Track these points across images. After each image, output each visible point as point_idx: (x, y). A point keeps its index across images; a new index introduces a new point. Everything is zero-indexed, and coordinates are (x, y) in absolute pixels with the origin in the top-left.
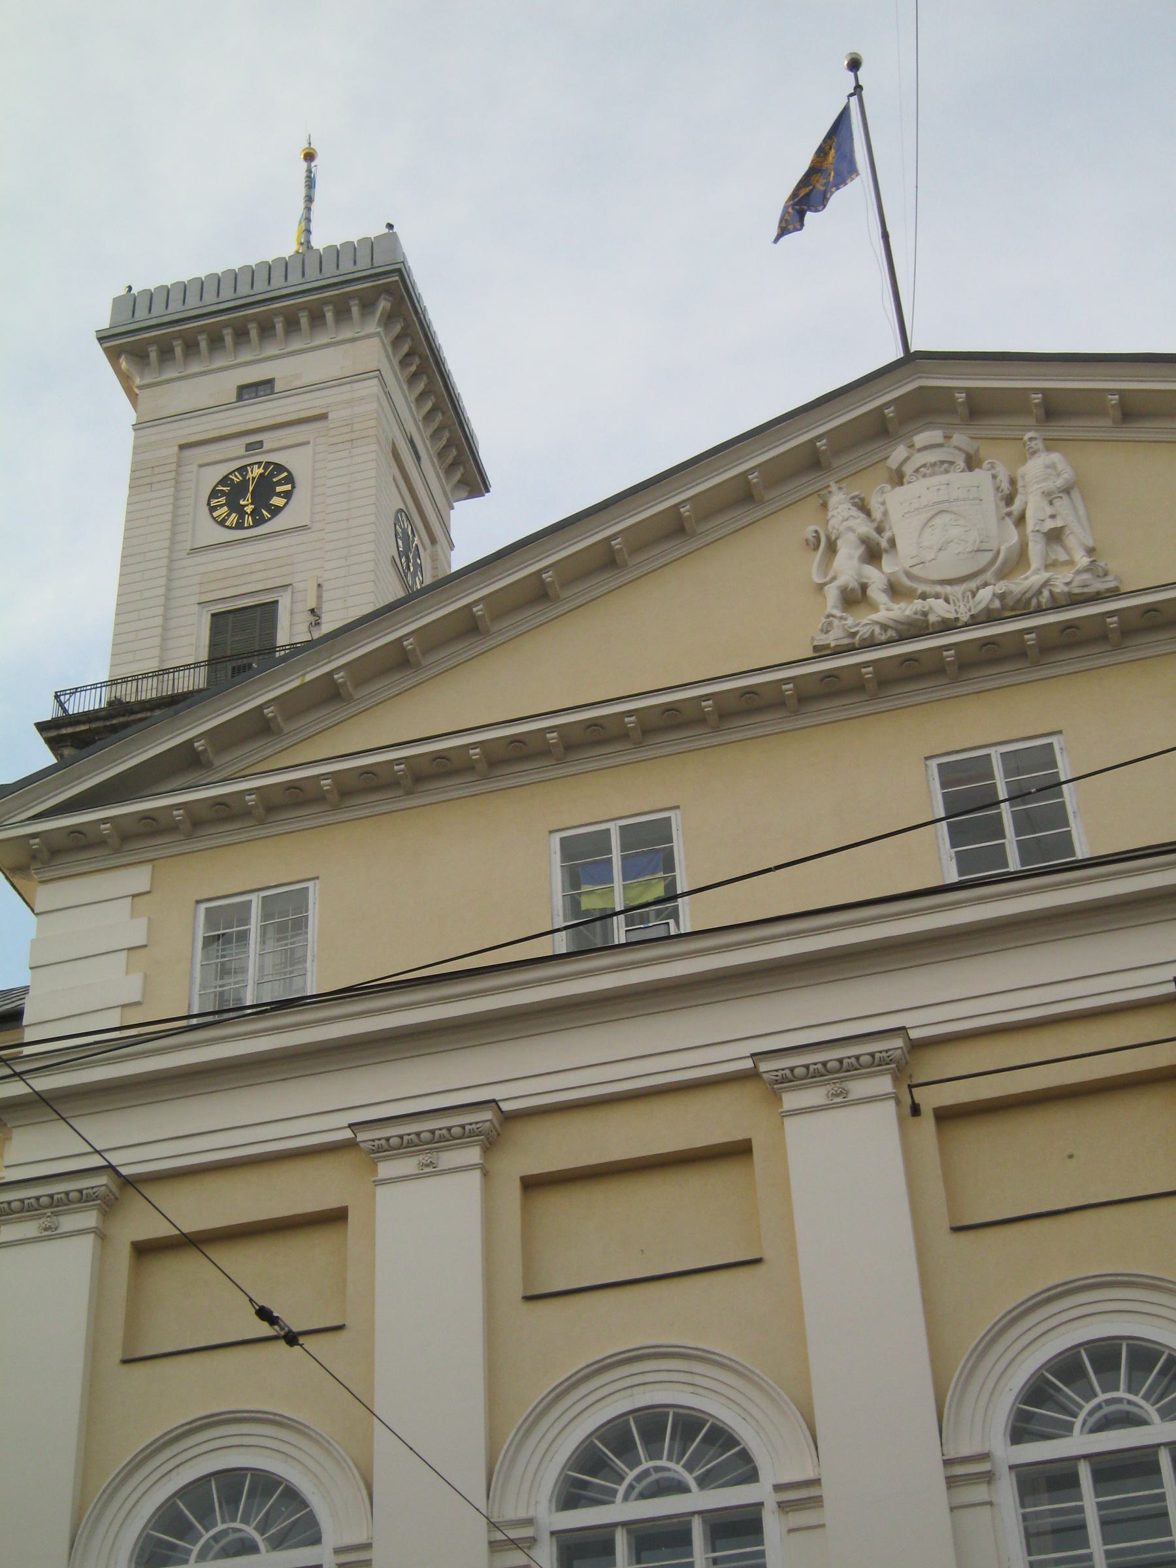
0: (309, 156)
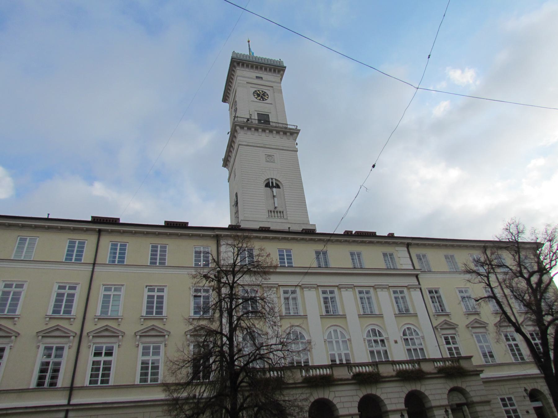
0: (249, 42)
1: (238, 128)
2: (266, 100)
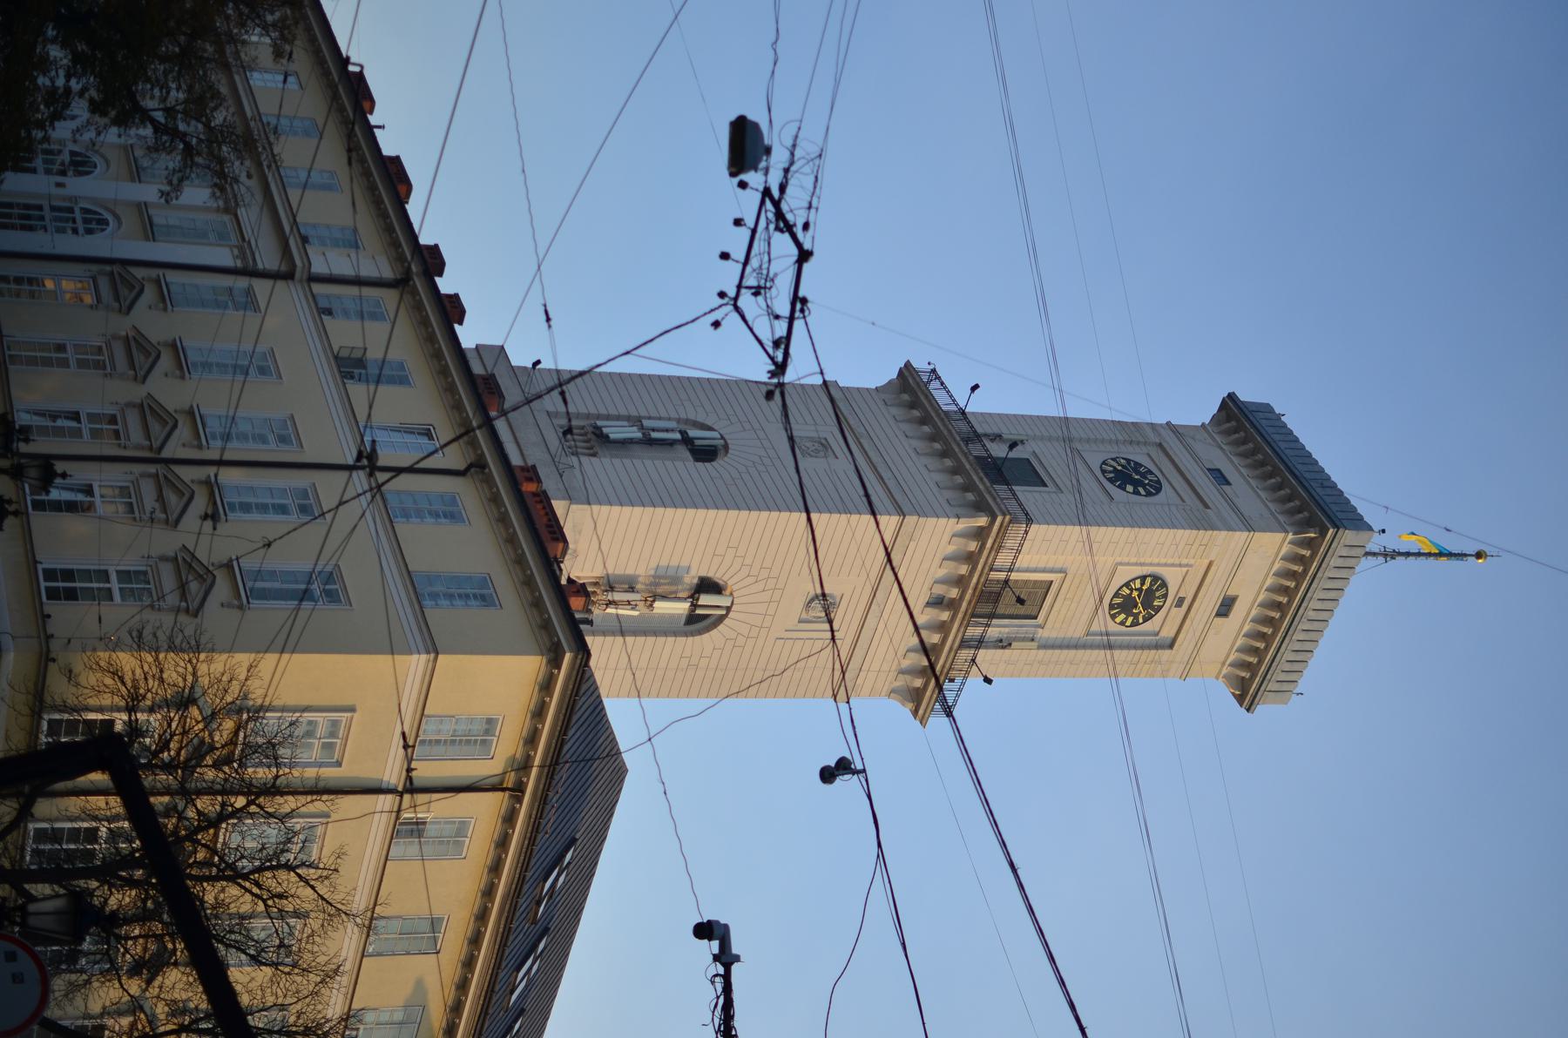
0: (1479, 555)
1: (982, 521)
2: (1113, 617)
